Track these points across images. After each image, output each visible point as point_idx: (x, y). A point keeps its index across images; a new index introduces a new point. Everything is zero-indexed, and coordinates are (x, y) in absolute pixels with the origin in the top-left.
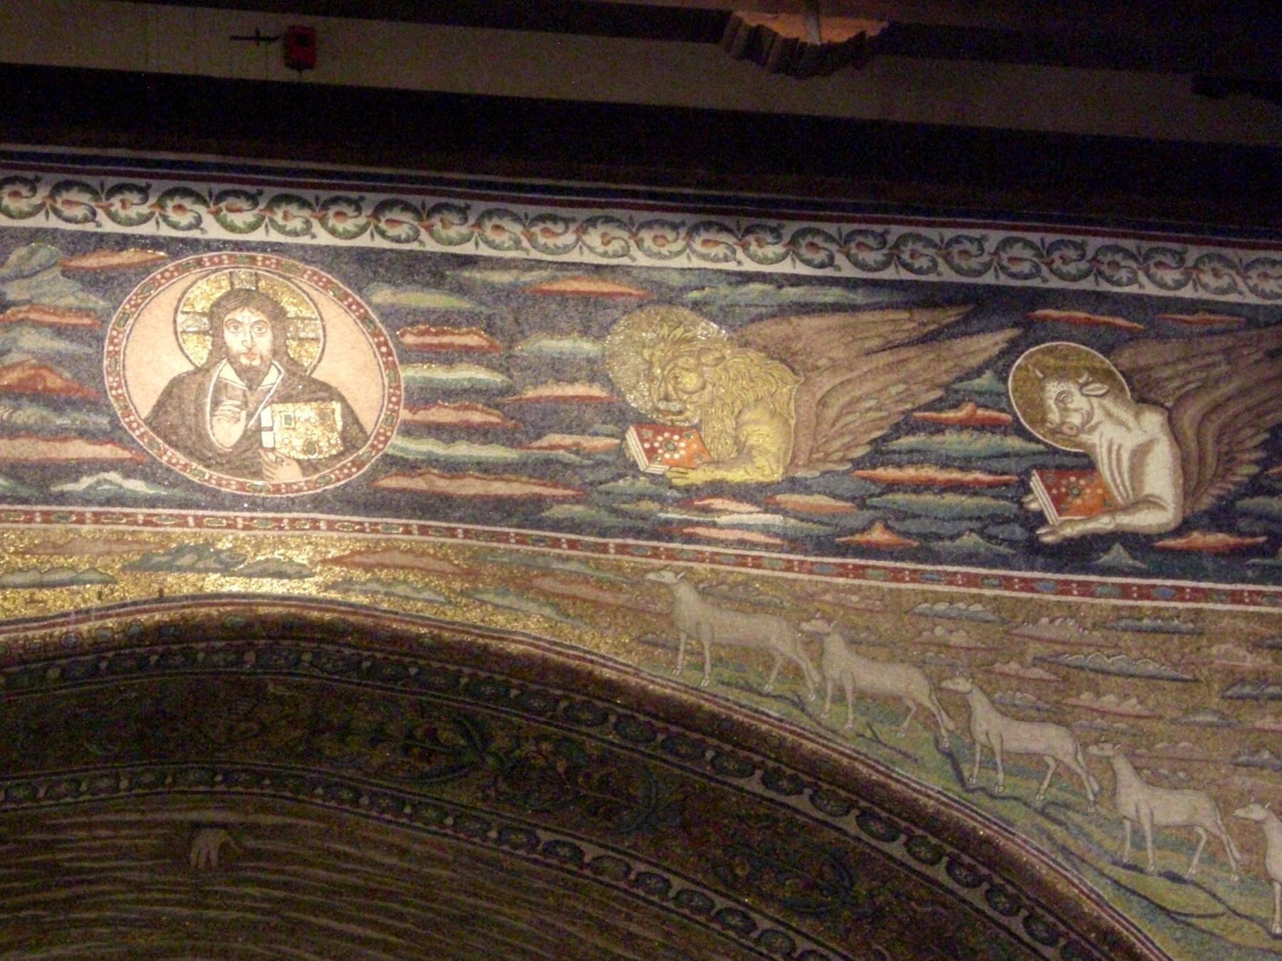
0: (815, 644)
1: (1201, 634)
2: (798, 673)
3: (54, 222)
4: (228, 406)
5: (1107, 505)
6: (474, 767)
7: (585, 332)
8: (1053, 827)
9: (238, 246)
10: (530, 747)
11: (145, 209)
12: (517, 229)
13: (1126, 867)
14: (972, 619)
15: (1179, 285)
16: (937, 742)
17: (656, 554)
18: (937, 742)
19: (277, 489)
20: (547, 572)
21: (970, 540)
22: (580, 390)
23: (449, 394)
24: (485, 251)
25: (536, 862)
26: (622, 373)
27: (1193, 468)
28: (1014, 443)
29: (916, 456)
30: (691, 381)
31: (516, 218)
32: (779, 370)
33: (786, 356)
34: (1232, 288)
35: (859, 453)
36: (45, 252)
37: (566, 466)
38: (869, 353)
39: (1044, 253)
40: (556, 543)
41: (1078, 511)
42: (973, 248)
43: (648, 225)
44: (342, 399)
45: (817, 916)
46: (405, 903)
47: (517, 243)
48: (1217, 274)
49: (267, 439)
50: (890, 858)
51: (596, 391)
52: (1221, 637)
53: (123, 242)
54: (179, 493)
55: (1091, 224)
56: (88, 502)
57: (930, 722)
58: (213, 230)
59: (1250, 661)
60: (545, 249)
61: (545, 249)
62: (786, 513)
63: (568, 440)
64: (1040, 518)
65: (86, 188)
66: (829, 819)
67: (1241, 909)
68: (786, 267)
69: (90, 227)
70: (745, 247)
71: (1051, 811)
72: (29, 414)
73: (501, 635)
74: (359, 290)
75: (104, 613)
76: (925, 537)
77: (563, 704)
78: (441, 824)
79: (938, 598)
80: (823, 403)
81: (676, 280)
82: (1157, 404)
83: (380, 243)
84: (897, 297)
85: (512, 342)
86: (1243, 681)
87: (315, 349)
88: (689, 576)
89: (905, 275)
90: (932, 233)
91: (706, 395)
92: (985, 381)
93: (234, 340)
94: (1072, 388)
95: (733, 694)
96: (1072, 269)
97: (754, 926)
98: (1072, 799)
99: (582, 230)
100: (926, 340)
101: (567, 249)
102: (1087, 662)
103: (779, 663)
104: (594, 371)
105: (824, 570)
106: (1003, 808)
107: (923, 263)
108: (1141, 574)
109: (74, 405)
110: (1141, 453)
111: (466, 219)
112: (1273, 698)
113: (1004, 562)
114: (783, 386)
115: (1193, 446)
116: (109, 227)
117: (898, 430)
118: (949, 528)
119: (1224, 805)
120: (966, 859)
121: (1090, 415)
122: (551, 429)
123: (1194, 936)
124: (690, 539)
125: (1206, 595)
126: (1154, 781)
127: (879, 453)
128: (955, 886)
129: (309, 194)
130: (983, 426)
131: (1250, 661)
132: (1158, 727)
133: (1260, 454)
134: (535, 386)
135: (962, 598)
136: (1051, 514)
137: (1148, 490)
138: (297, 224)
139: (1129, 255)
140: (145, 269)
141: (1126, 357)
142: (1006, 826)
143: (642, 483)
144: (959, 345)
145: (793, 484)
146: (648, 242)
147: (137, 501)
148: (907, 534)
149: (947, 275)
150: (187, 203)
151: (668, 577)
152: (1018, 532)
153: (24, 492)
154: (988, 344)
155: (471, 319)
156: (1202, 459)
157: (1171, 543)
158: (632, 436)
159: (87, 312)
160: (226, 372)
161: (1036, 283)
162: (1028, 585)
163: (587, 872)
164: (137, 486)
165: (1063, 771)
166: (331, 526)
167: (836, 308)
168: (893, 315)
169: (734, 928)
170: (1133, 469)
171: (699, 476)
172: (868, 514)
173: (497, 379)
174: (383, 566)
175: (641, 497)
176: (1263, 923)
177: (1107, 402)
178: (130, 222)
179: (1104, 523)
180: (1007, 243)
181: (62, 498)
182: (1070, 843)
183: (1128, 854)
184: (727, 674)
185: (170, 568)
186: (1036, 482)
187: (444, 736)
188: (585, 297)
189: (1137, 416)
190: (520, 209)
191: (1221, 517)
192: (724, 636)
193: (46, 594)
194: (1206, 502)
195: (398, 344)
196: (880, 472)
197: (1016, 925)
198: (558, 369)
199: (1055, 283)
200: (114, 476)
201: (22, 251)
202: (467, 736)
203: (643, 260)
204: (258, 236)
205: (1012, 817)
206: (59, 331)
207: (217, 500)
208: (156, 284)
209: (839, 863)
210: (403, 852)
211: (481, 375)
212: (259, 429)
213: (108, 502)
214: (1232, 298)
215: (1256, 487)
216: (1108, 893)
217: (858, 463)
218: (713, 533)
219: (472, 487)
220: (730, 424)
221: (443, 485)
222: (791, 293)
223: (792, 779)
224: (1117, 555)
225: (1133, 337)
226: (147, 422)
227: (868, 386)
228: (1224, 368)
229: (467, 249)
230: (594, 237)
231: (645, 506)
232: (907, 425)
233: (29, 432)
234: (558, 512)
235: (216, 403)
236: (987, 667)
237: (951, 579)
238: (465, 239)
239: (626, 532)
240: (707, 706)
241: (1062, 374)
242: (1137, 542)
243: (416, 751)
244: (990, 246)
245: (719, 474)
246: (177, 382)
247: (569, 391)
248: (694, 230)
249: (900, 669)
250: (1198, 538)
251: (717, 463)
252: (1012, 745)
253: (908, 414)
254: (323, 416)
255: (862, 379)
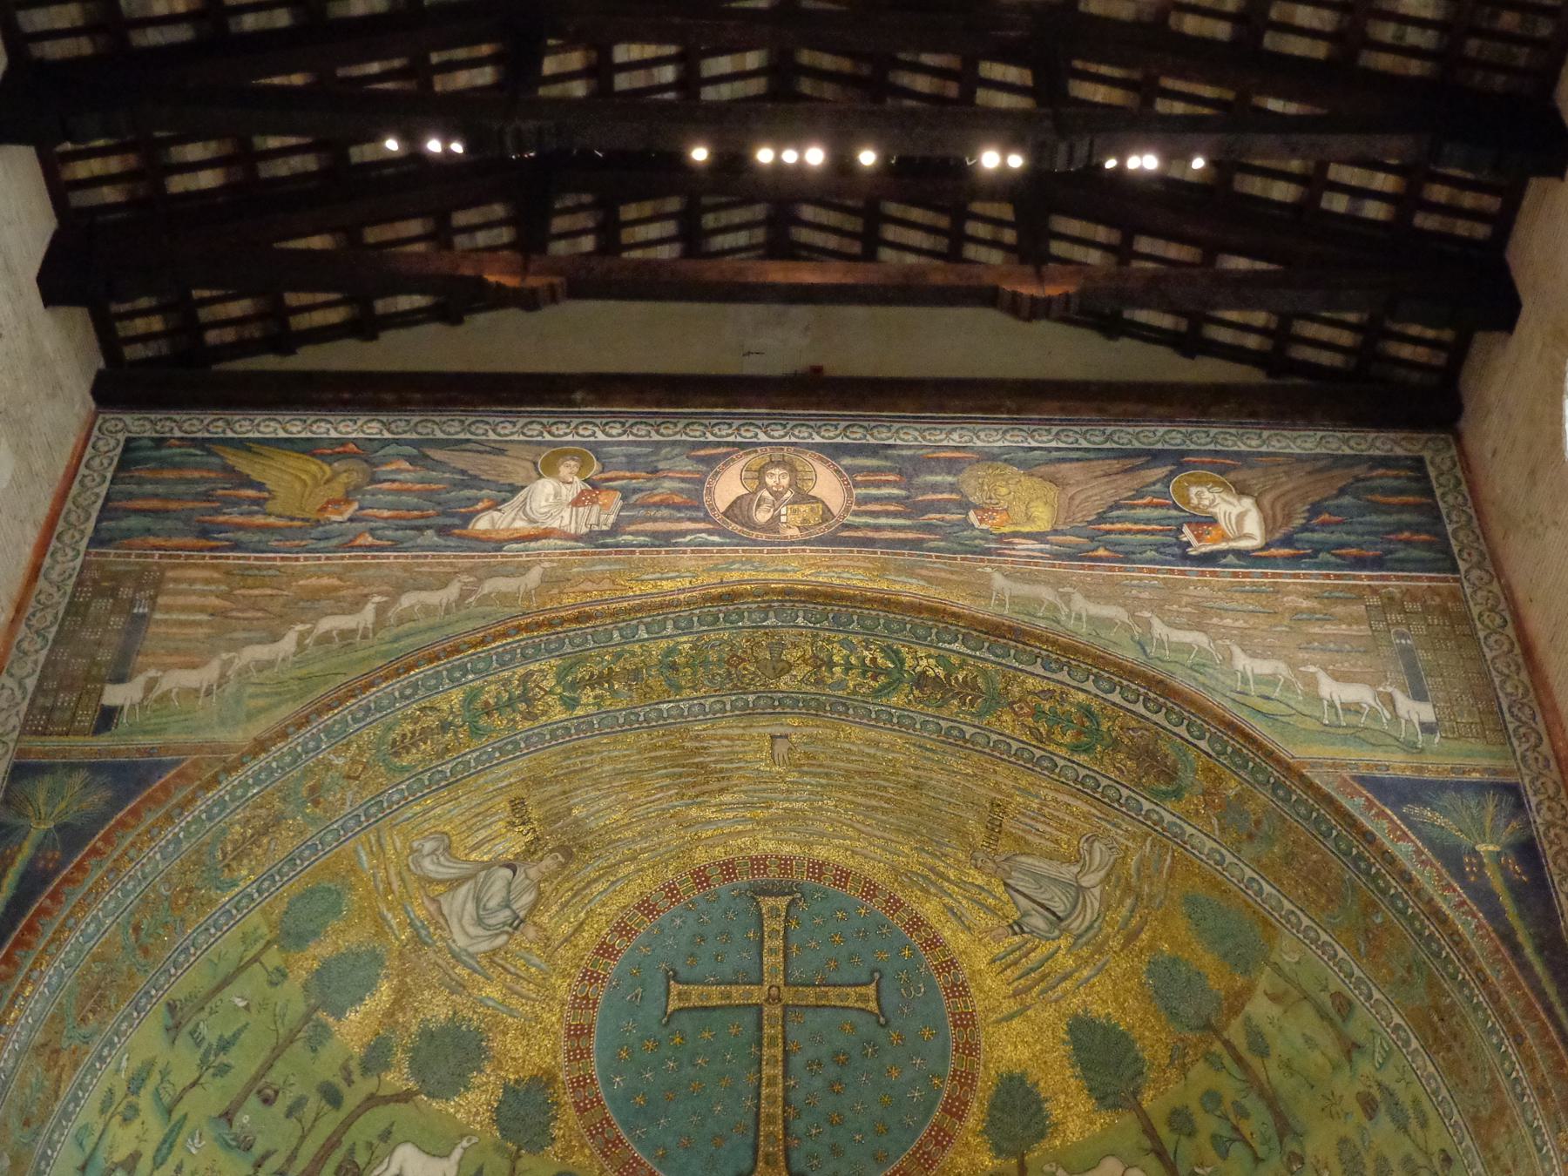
0: (1067, 599)
1: (1278, 592)
2: (1056, 609)
3: (684, 438)
4: (764, 506)
5: (1225, 538)
6: (900, 681)
7: (949, 473)
8: (1197, 675)
9: (776, 444)
10: (924, 663)
11: (730, 431)
12: (916, 434)
13: (1240, 693)
14: (1153, 587)
15: (1260, 446)
16: (1132, 638)
17: (982, 561)
18: (1132, 638)
19: (786, 537)
20: (922, 567)
21: (1150, 554)
22: (946, 496)
23: (877, 499)
24: (899, 442)
25: (943, 742)
26: (965, 489)
27: (1270, 521)
28: (1174, 513)
29: (1119, 519)
30: (1004, 491)
31: (916, 430)
32: (1048, 484)
33: (1053, 480)
34: (1289, 447)
35: (1090, 519)
36: (677, 451)
37: (937, 526)
38: (1096, 477)
39: (1188, 436)
40: (930, 557)
41: (1208, 541)
42: (1151, 435)
43: (984, 430)
44: (823, 502)
45: (1085, 751)
46: (884, 780)
47: (916, 439)
48: (1279, 441)
49: (783, 519)
50: (1114, 704)
51: (954, 496)
52: (1288, 594)
53: (719, 444)
54: (735, 541)
55: (1211, 424)
56: (687, 545)
57: (1129, 628)
58: (763, 438)
59: (1305, 604)
60: (930, 441)
61: (930, 441)
62: (1052, 544)
63: (938, 516)
64: (1189, 544)
65: (702, 424)
66: (1080, 685)
67: (1307, 712)
68: (1054, 444)
69: (702, 439)
70: (1033, 437)
71: (1196, 668)
72: (665, 512)
73: (897, 593)
74: (834, 459)
75: (693, 589)
76: (1127, 553)
77: (934, 631)
78: (891, 722)
79: (1133, 578)
80: (1072, 498)
81: (996, 451)
82: (1249, 495)
83: (846, 440)
84: (1110, 454)
85: (911, 477)
86: (1302, 612)
87: (810, 484)
88: (999, 569)
89: (1115, 446)
90: (1130, 430)
91: (1011, 496)
92: (1158, 487)
93: (770, 481)
94: (1204, 489)
95: (1021, 617)
96: (1203, 441)
97: (1056, 766)
98: (1208, 662)
99: (950, 432)
100: (1125, 471)
101: (941, 440)
102: (1216, 605)
103: (1046, 603)
104: (953, 488)
105: (1071, 567)
106: (1170, 667)
107: (1125, 441)
108: (1242, 567)
109: (688, 508)
110: (1241, 517)
111: (890, 431)
112: (1318, 620)
113: (1170, 563)
114: (1052, 492)
115: (1270, 512)
116: (711, 438)
117: (1111, 508)
118: (1138, 549)
119: (1293, 665)
120: (1152, 695)
121: (1214, 500)
122: (929, 512)
123: (1279, 724)
124: (1000, 555)
125: (1280, 576)
126: (1254, 655)
127: (1101, 518)
128: (1148, 714)
129: (812, 423)
130: (1157, 506)
131: (1305, 604)
132: (1256, 633)
133: (1306, 515)
134: (923, 494)
135: (1146, 578)
136: (1194, 542)
137: (1245, 531)
138: (806, 435)
139: (1231, 435)
140: (728, 454)
141: (1233, 476)
142: (1172, 675)
143: (976, 533)
144: (1143, 473)
145: (1055, 532)
146: (982, 435)
147: (714, 544)
148: (1116, 552)
149: (1137, 445)
150: (751, 428)
151: (988, 570)
152: (1176, 550)
153: (657, 543)
154: (1160, 472)
155: (891, 470)
156: (1274, 516)
157: (1260, 554)
158: (972, 514)
159: (698, 472)
160: (766, 493)
161: (1184, 447)
162: (1182, 573)
163: (969, 745)
164: (716, 539)
165: (1201, 650)
166: (811, 551)
167: (1078, 460)
168: (1108, 462)
169: (1046, 768)
170: (1237, 523)
171: (1006, 530)
172: (1096, 544)
173: (904, 493)
174: (837, 566)
175: (976, 538)
176: (1318, 719)
177: (1224, 495)
178: (721, 436)
179: (1223, 546)
180: (1166, 433)
181: (675, 545)
182: (1207, 682)
183: (1239, 687)
184: (1017, 609)
185: (727, 570)
186: (1186, 529)
187: (880, 661)
188: (950, 460)
189: (1239, 500)
190: (918, 426)
191: (1287, 541)
192: (1015, 593)
193: (664, 583)
194: (1277, 536)
195: (853, 481)
196: (1103, 526)
197: (1182, 731)
198: (934, 488)
199: (1193, 447)
200: (704, 535)
201: (668, 449)
202: (893, 662)
203: (979, 444)
204: (786, 439)
205: (1174, 670)
206: (683, 480)
207: (755, 543)
208: (733, 460)
209: (1087, 712)
210: (877, 744)
211: (896, 491)
212: (780, 515)
213: (700, 545)
214: (1287, 451)
215: (1304, 529)
216: (1229, 705)
217: (1090, 523)
218: (1013, 552)
219: (888, 535)
220: (1023, 508)
221: (870, 534)
222: (1055, 454)
223: (1057, 661)
224: (1231, 559)
225: (1235, 468)
226: (724, 514)
227: (1096, 491)
228: (1284, 479)
229: (891, 442)
230: (955, 436)
231: (977, 542)
232: (1117, 506)
233: (663, 519)
234: (932, 544)
235: (758, 506)
236: (1161, 607)
237: (1141, 570)
238: (889, 438)
239: (966, 553)
240: (1007, 623)
241: (1199, 483)
242: (1241, 554)
243: (869, 674)
244: (1159, 434)
245: (1018, 529)
246: (738, 498)
247: (940, 496)
248: (1005, 432)
249: (1114, 608)
250: (1273, 551)
251: (1016, 524)
252: (1174, 639)
253: (1116, 502)
254: (812, 510)
255: (1093, 487)
